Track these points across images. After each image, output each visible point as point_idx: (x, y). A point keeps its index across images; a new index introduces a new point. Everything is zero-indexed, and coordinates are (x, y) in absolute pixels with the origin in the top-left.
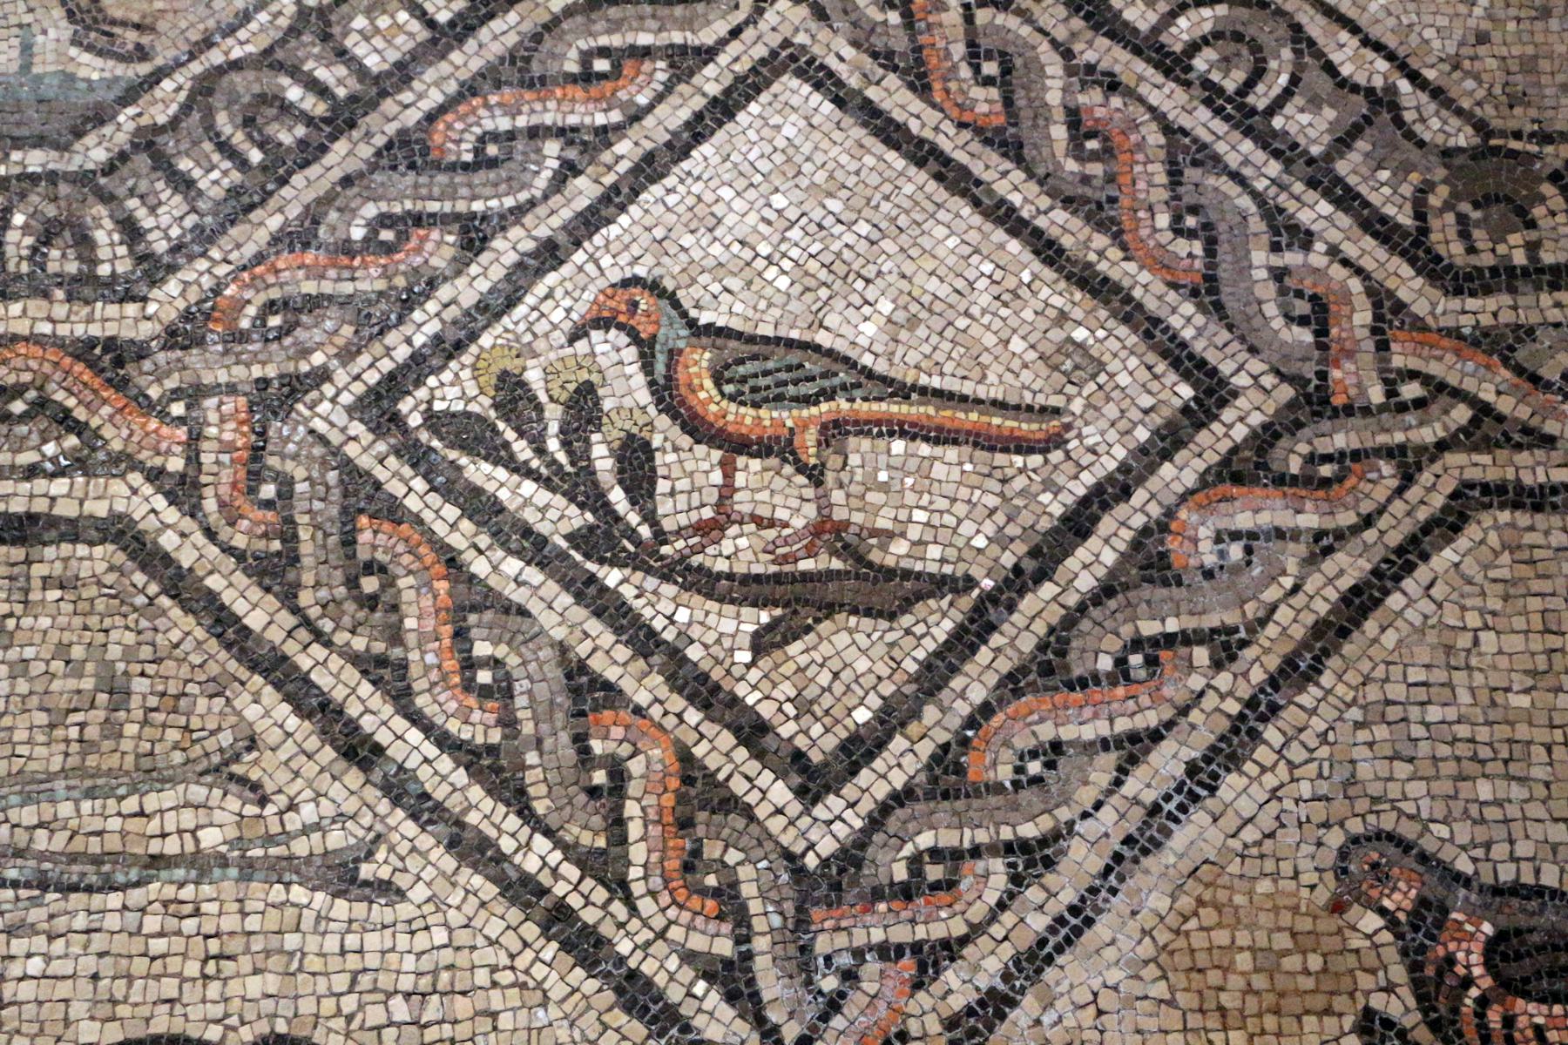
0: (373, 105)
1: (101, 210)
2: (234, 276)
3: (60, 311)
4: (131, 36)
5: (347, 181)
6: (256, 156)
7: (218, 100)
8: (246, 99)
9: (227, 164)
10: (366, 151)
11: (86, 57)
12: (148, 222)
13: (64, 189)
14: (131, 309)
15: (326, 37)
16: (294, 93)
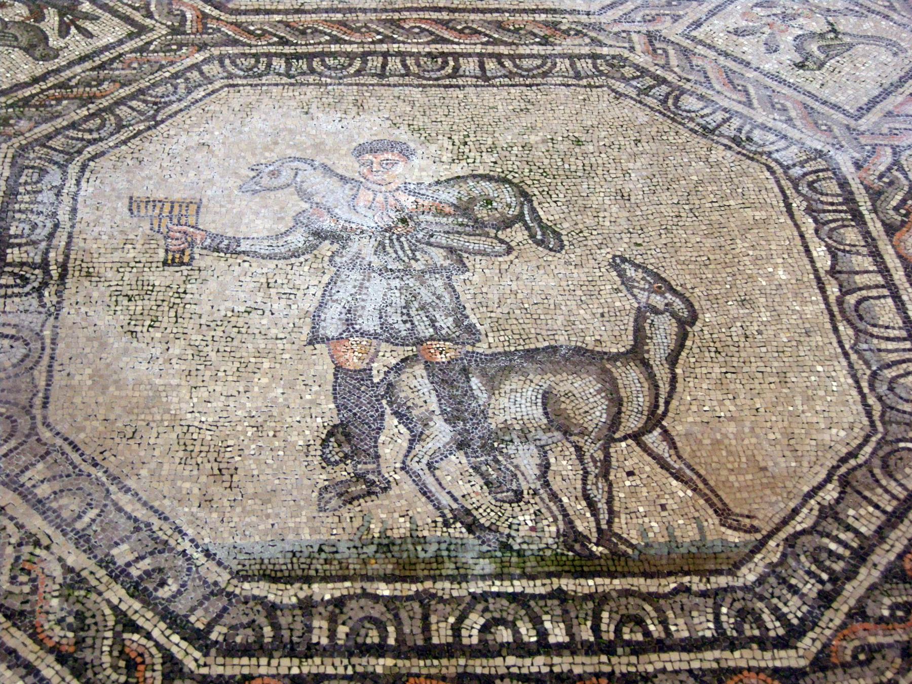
0: (871, 550)
1: (760, 605)
2: (834, 636)
3: (758, 653)
4: (747, 521)
5: (872, 588)
6: (825, 576)
7: (798, 550)
8: (811, 550)
9: (813, 581)
10: (876, 574)
11: (729, 532)
12: (785, 610)
13: (740, 594)
14: (792, 652)
15: (836, 518)
16: (833, 546)
